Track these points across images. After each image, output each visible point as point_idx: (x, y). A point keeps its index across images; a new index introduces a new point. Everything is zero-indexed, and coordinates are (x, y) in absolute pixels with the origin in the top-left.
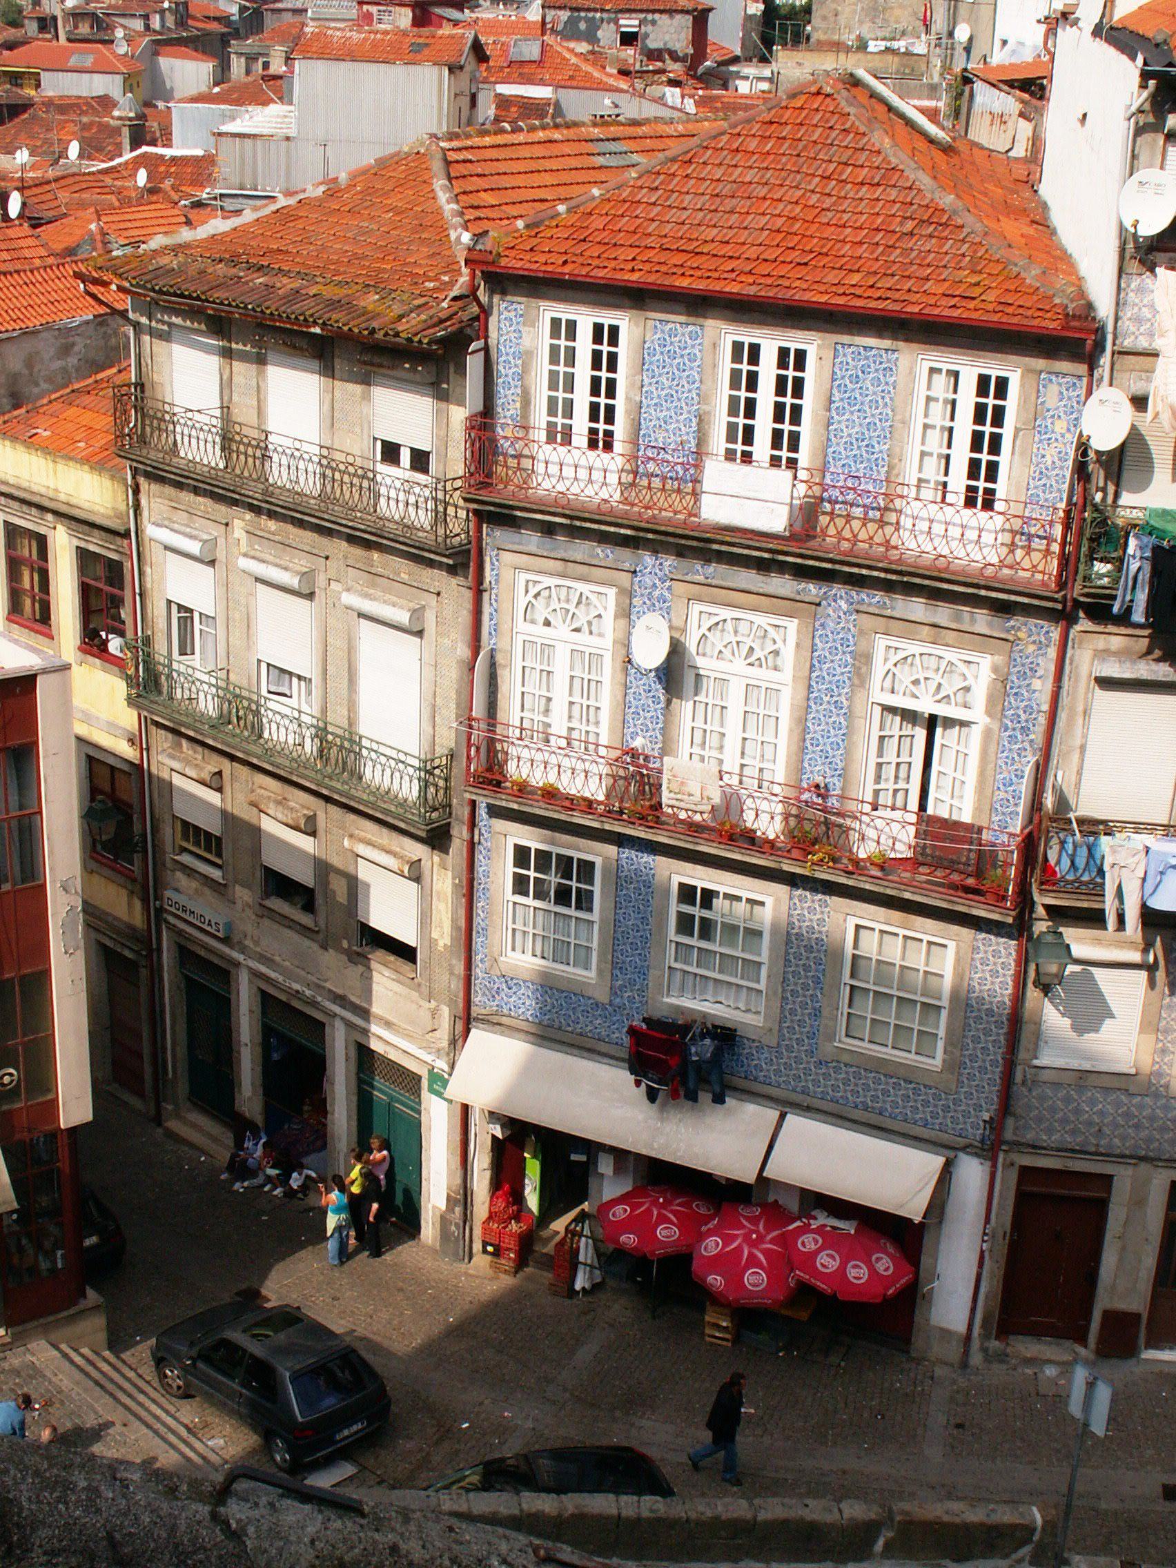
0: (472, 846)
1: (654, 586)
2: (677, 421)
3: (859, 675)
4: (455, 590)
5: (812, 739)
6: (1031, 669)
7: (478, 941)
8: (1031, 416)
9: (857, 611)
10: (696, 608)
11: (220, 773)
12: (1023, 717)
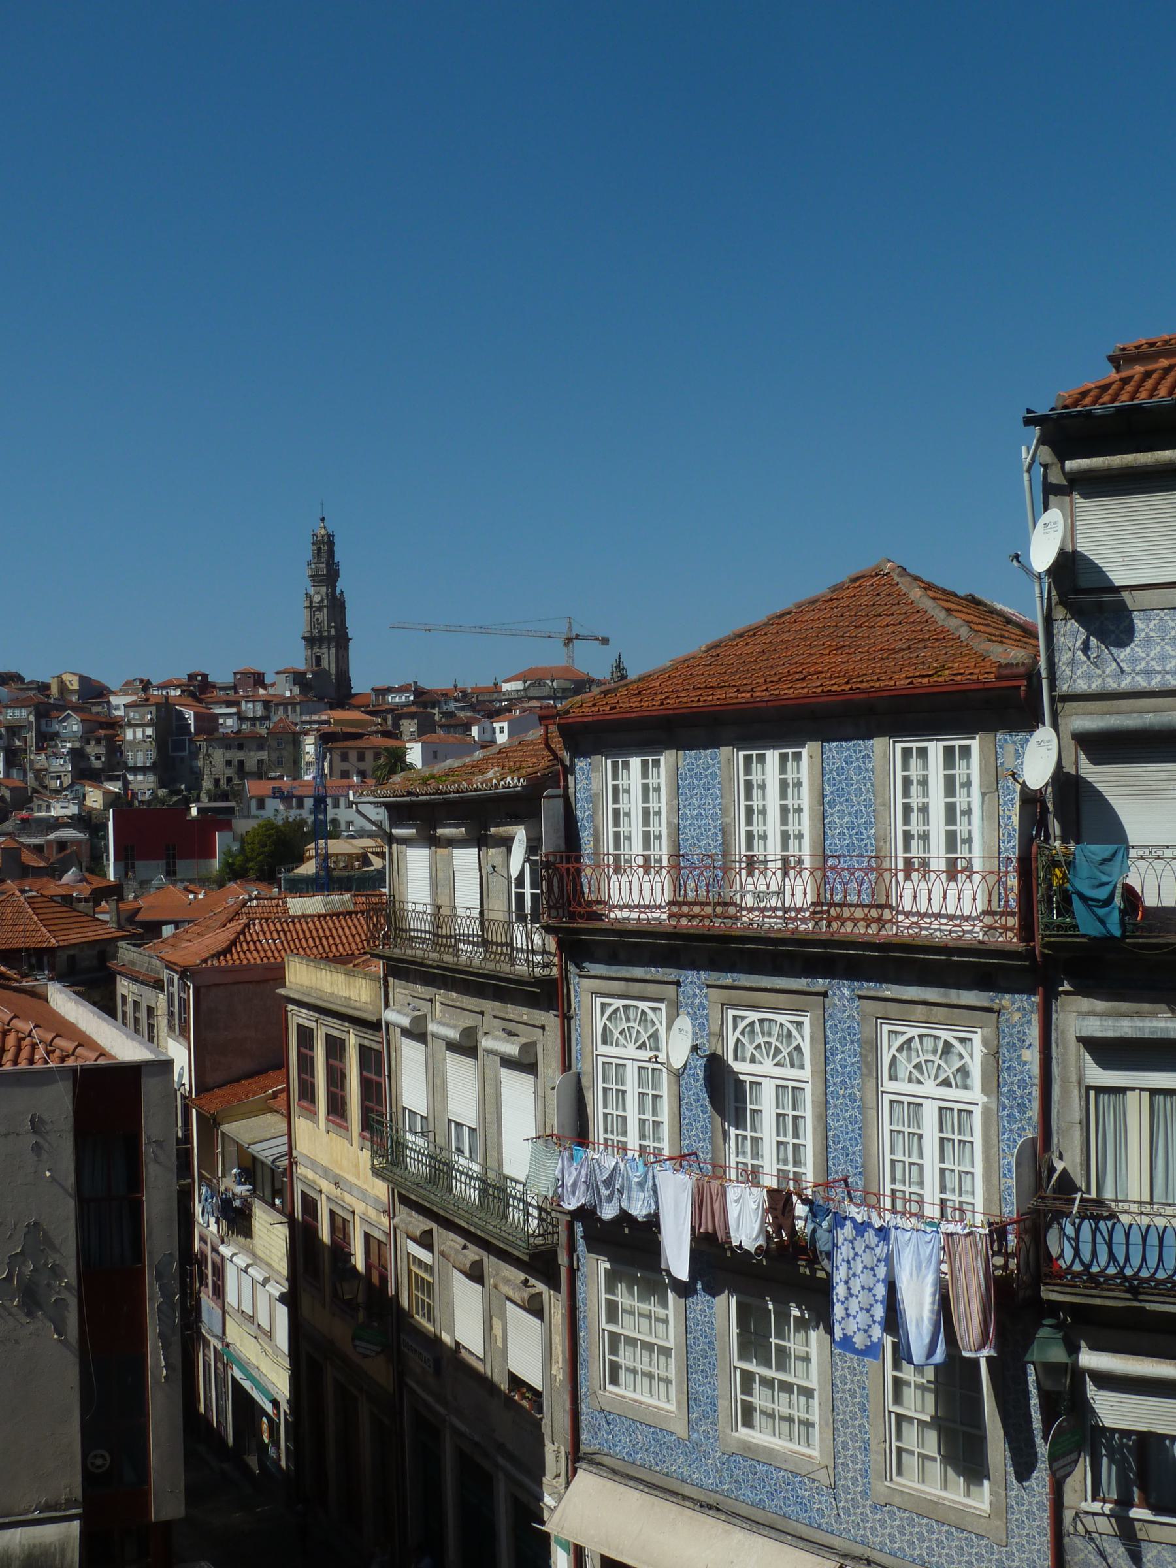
0: (573, 1272)
1: (695, 995)
2: (707, 837)
3: (867, 1064)
4: (550, 1019)
5: (834, 1136)
6: (1019, 1040)
7: (582, 1372)
8: (993, 779)
9: (860, 997)
10: (731, 1013)
11: (430, 1232)
12: (1018, 1092)
